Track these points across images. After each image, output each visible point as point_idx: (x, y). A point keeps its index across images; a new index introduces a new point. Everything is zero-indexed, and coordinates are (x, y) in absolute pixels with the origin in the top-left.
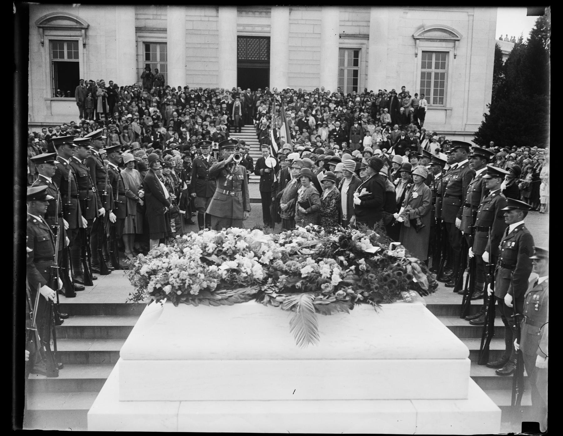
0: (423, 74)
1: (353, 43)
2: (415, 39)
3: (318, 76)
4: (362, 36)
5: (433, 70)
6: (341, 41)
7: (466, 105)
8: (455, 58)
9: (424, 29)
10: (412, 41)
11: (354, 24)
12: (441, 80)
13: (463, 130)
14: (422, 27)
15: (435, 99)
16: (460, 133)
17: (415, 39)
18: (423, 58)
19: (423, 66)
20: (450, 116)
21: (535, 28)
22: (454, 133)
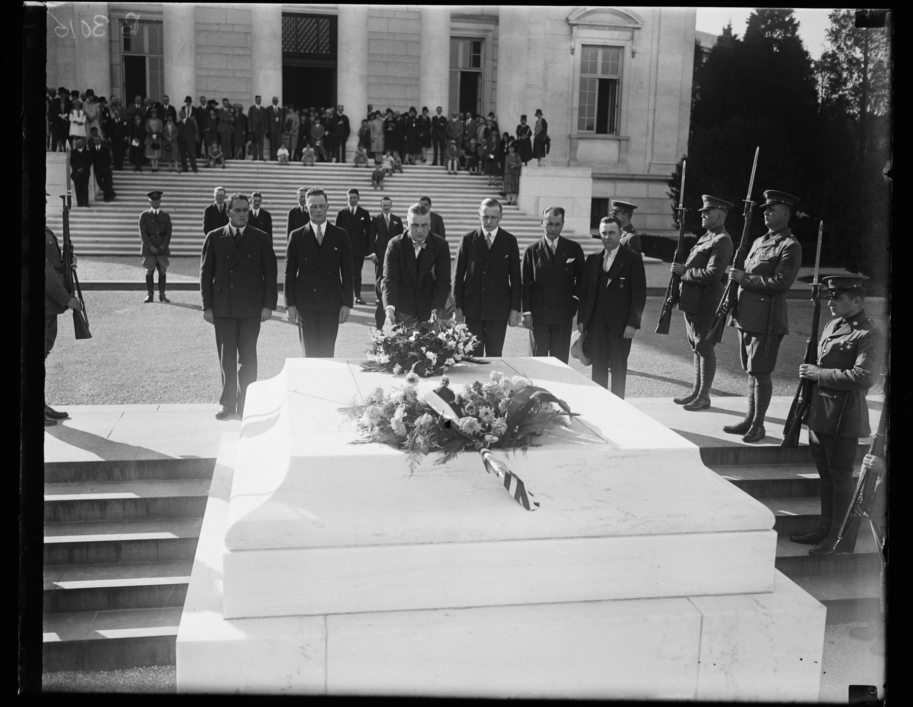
2: (572, 26)
3: (415, 82)
4: (485, 18)
7: (650, 131)
8: (633, 57)
10: (566, 29)
13: (646, 173)
16: (640, 177)
17: (572, 26)
22: (632, 177)
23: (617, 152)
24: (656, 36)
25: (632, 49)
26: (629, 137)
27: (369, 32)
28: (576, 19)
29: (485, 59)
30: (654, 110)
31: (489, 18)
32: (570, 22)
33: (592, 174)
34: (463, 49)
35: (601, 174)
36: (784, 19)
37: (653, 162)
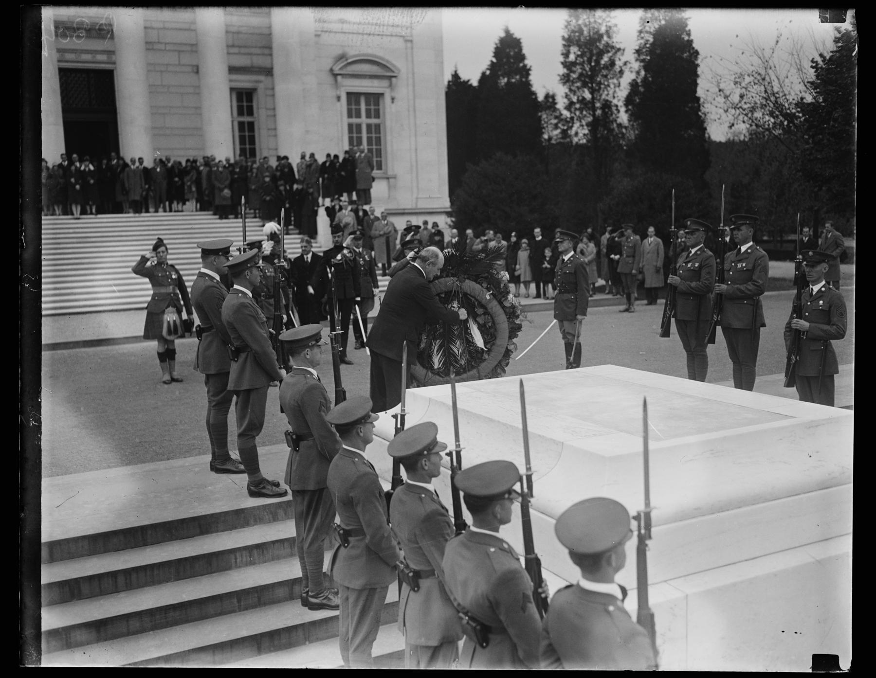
0: (350, 126)
1: (245, 81)
2: (335, 76)
3: (198, 132)
5: (364, 120)
6: (234, 77)
10: (330, 79)
11: (243, 50)
13: (414, 206)
14: (342, 57)
16: (410, 211)
17: (335, 76)
18: (349, 103)
19: (350, 116)
21: (494, 60)
22: (402, 211)
24: (411, 81)
26: (396, 175)
27: (150, 85)
30: (416, 150)
31: (258, 70)
32: (335, 72)
34: (239, 99)
36: (518, 65)
37: (420, 196)
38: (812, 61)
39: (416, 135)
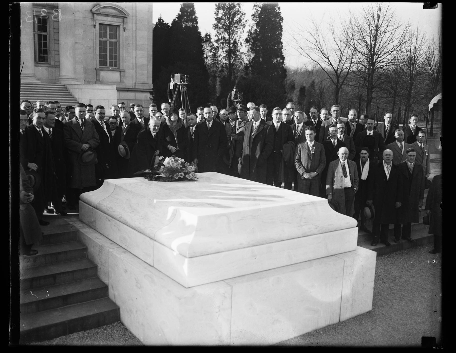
0: (100, 42)
2: (94, 14)
5: (108, 39)
7: (134, 68)
9: (100, 6)
10: (90, 15)
12: (115, 47)
13: (134, 87)
15: (111, 63)
16: (131, 90)
17: (94, 14)
18: (100, 29)
19: (100, 36)
20: (124, 76)
21: (180, 13)
22: (127, 89)
23: (119, 77)
24: (134, 21)
25: (124, 27)
26: (124, 70)
28: (95, 11)
29: (49, 28)
30: (136, 57)
32: (93, 12)
33: (116, 88)
35: (144, 89)
36: (192, 17)
38: (215, 13)
39: (136, 50)
